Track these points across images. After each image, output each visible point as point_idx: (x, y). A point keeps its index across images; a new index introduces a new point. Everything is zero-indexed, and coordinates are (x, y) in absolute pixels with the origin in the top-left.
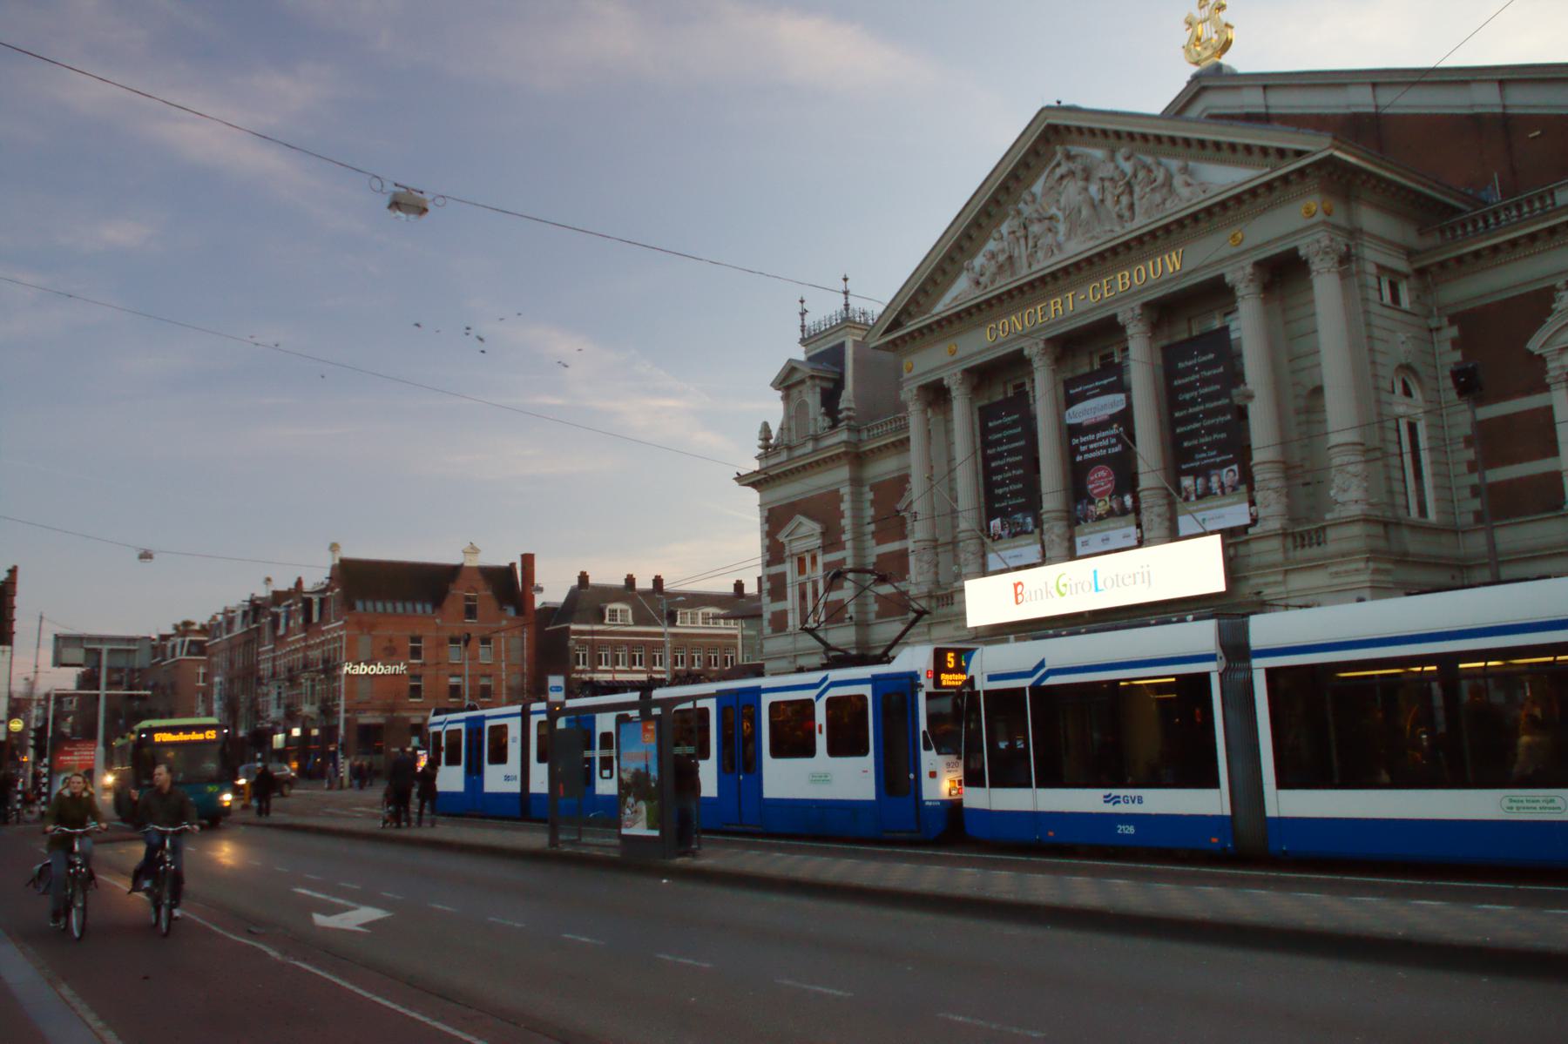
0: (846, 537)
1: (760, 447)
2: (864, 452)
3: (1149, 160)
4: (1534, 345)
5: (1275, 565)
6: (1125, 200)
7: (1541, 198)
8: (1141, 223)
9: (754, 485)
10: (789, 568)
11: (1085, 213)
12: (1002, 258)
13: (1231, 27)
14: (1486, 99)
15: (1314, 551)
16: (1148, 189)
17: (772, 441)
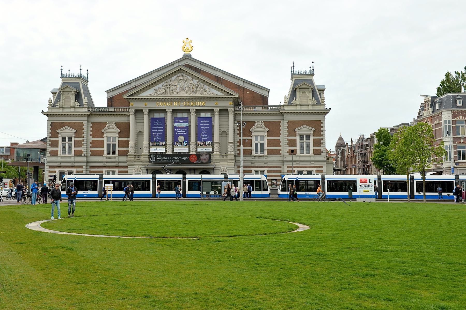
0: (84, 135)
1: (48, 104)
2: (92, 115)
3: (202, 84)
4: (251, 130)
5: (219, 160)
6: (195, 89)
7: (254, 107)
8: (198, 95)
9: (47, 115)
10: (60, 139)
11: (187, 89)
12: (164, 91)
13: (192, 47)
14: (241, 84)
15: (225, 158)
16: (202, 90)
17: (52, 103)
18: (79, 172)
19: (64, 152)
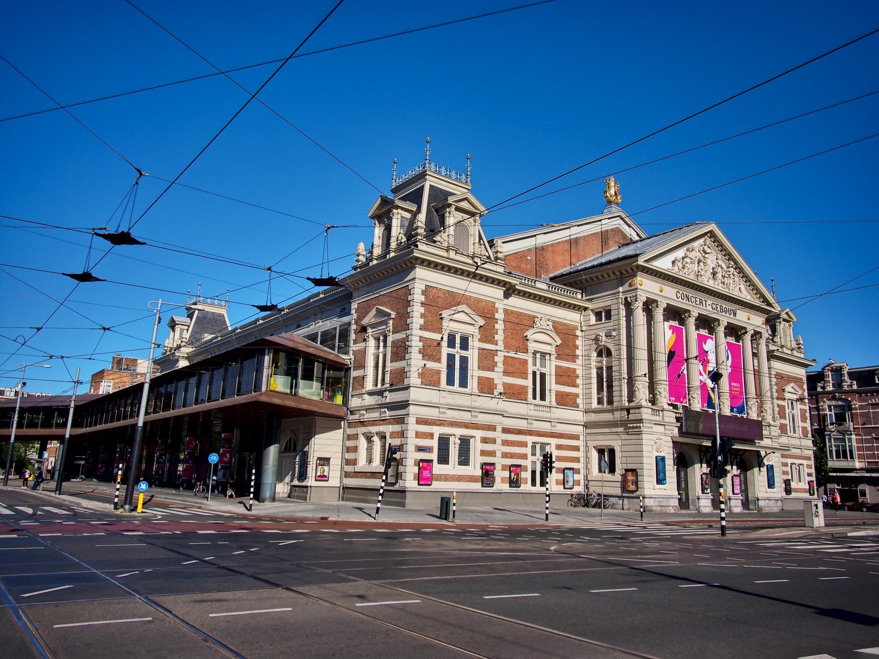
18: (486, 440)
19: (450, 382)
